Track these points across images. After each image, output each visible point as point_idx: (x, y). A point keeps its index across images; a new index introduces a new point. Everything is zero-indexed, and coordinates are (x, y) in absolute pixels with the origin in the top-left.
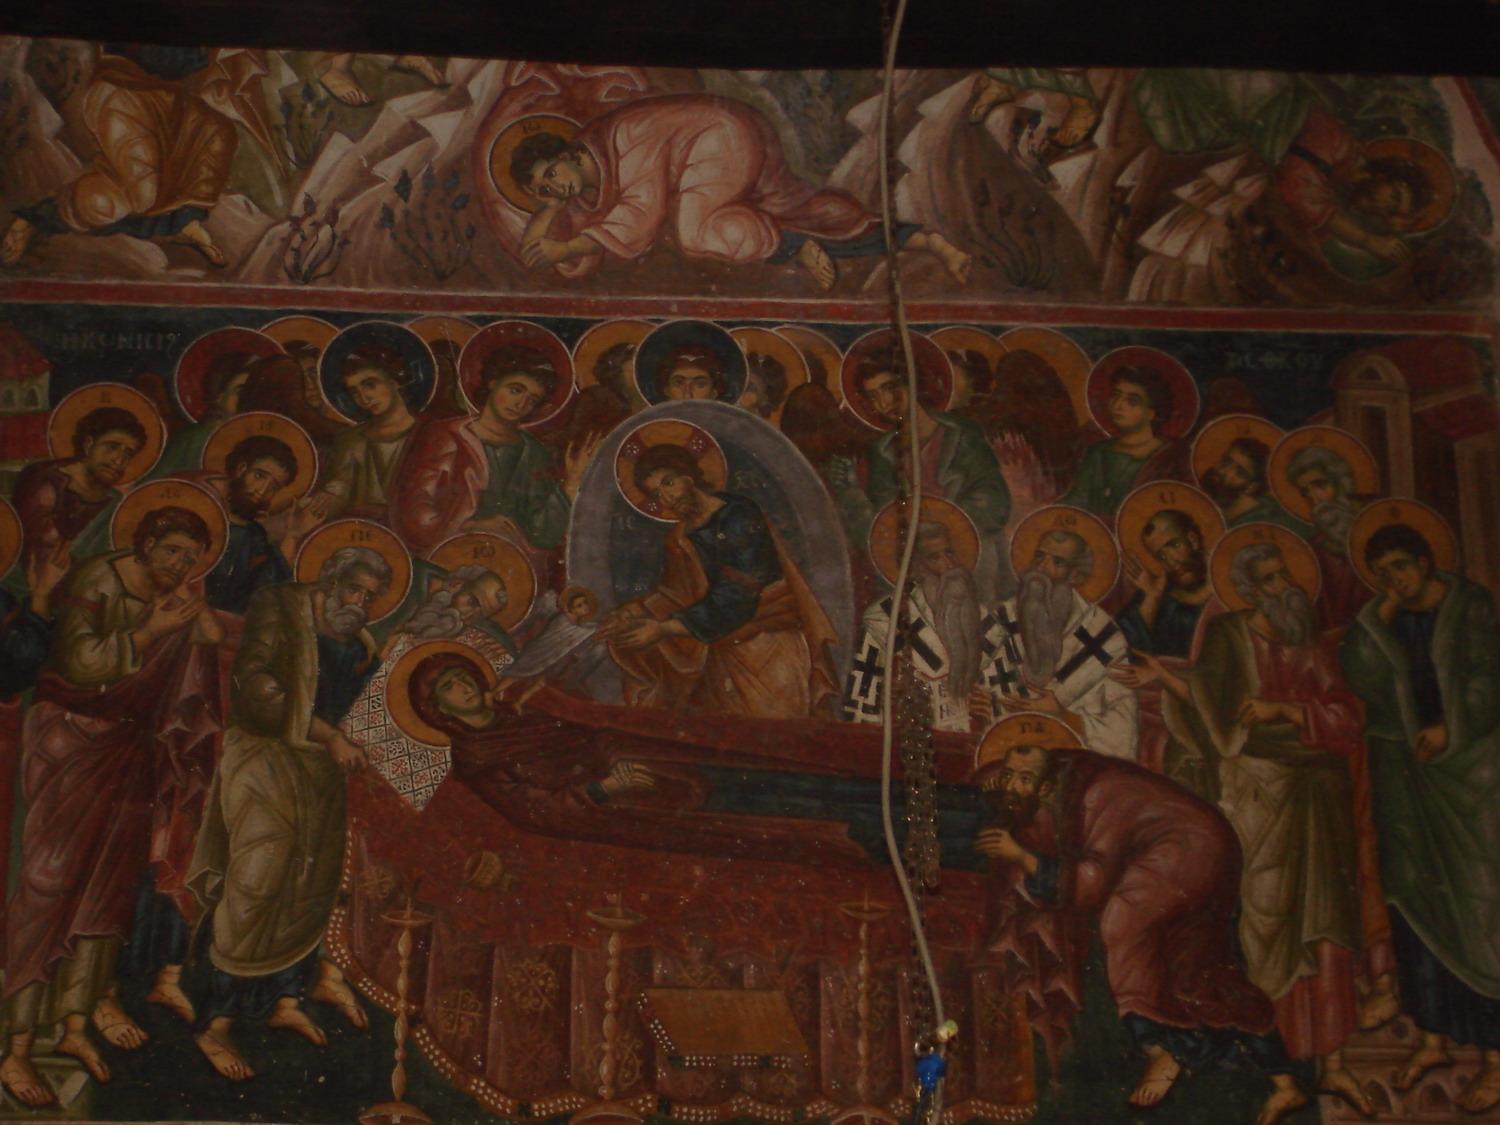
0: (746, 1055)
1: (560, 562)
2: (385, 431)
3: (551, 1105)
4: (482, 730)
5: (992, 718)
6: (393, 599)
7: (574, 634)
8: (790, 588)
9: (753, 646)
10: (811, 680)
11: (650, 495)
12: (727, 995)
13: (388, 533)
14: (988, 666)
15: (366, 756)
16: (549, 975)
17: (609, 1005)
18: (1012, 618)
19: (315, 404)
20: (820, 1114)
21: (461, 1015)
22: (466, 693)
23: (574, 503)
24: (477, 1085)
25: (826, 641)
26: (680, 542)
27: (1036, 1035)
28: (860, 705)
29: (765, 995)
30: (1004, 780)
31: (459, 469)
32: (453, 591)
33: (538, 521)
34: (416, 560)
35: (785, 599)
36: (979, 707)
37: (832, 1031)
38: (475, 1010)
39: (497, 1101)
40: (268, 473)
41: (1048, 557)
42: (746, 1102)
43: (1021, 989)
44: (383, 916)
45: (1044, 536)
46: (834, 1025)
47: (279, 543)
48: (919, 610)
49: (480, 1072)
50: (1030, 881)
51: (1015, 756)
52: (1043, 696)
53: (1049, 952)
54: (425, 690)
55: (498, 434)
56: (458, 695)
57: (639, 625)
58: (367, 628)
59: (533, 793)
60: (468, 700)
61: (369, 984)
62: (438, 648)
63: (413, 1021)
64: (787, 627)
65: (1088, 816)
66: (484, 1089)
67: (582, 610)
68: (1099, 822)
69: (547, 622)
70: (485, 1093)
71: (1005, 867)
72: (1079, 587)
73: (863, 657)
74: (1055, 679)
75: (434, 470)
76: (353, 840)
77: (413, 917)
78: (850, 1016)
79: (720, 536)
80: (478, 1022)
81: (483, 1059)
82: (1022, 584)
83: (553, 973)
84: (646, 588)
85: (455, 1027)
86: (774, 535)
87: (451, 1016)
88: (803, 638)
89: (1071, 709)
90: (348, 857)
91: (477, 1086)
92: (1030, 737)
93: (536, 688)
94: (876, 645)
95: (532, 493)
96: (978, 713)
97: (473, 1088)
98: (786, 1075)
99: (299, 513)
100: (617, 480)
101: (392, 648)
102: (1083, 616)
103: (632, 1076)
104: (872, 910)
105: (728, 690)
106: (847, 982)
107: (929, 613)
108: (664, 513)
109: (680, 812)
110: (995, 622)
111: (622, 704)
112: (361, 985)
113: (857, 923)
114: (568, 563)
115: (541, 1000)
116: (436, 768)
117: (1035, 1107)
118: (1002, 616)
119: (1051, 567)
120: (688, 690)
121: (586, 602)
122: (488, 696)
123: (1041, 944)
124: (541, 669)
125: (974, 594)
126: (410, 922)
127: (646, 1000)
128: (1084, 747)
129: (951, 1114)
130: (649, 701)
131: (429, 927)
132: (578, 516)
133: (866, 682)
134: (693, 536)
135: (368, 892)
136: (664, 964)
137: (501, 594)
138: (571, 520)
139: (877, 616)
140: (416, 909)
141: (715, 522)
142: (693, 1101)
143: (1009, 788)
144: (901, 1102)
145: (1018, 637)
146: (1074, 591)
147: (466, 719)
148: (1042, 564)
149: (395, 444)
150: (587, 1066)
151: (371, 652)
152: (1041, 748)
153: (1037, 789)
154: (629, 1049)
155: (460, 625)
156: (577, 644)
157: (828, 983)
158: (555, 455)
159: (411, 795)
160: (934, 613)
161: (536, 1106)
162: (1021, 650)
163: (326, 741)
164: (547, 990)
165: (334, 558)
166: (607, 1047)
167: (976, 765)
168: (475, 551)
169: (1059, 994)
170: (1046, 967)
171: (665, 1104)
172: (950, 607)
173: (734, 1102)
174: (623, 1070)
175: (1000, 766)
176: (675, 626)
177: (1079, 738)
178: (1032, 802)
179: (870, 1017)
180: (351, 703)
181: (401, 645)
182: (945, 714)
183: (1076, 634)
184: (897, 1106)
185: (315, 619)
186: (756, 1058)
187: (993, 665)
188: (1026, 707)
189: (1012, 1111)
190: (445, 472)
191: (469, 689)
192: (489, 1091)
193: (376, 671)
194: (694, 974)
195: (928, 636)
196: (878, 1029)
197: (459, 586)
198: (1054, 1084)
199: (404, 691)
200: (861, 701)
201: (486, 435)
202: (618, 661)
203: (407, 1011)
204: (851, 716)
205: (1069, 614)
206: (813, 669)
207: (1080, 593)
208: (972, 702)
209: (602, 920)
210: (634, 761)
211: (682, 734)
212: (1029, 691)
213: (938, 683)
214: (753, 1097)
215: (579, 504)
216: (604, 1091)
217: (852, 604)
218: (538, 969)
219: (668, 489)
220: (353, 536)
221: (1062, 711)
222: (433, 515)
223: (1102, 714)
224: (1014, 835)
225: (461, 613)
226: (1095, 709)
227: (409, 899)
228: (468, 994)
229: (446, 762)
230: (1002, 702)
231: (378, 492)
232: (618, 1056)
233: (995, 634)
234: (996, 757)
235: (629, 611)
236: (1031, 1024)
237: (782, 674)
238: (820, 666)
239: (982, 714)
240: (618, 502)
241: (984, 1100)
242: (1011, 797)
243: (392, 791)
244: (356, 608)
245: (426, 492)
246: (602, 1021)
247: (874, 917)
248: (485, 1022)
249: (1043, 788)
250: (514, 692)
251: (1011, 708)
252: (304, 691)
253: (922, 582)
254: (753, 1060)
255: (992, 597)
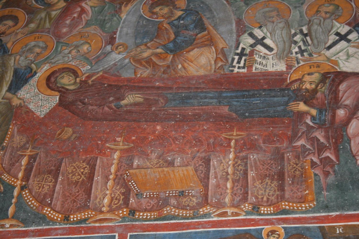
0: (173, 191)
1: (115, 36)
2: (55, 8)
3: (79, 216)
4: (74, 90)
5: (296, 65)
6: (46, 54)
7: (116, 57)
8: (209, 33)
9: (192, 53)
10: (215, 61)
11: (154, 13)
12: (166, 169)
13: (49, 36)
14: (295, 48)
15: (24, 102)
16: (86, 167)
17: (111, 177)
18: (305, 32)
19: (30, 4)
20: (206, 212)
21: (44, 185)
22: (70, 79)
23: (123, 19)
24: (47, 211)
25: (223, 48)
26: (164, 25)
27: (316, 175)
28: (237, 67)
29: (184, 168)
30: (301, 85)
31: (80, 16)
32: (70, 49)
33: (108, 25)
34: (58, 42)
35: (206, 37)
36: (290, 62)
37: (215, 180)
38: (50, 182)
39: (55, 216)
40: (7, 24)
41: (322, 12)
42: (171, 209)
43: (309, 158)
44: (18, 152)
45: (320, 6)
46: (216, 177)
47: (6, 44)
48: (264, 34)
49: (49, 205)
50: (313, 118)
51: (306, 76)
52: (320, 56)
53: (323, 143)
54: (53, 79)
55: (97, 4)
56: (67, 81)
57: (144, 52)
58: (34, 64)
59: (90, 107)
60: (69, 81)
61: (6, 176)
62: (61, 67)
63: (23, 188)
64: (206, 45)
65: (341, 94)
66: (50, 212)
67: (121, 50)
68: (346, 94)
69: (107, 54)
70: (50, 213)
71: (301, 115)
72: (336, 20)
73: (239, 51)
74: (325, 50)
75: (70, 16)
76: (12, 129)
77: (31, 151)
78: (224, 174)
79: (182, 22)
80: (51, 186)
81: (51, 201)
82: (310, 21)
83: (88, 167)
84: (148, 40)
85: (41, 189)
86: (204, 19)
87: (40, 185)
88: (213, 48)
89: (333, 58)
90: (8, 134)
91: (47, 211)
92: (313, 70)
93: (98, 75)
94: (244, 47)
95: (107, 18)
96: (290, 64)
97: (45, 211)
98: (191, 198)
99: (17, 34)
100: (142, 11)
101: (43, 68)
102: (338, 28)
103: (118, 203)
104: (237, 135)
105: (179, 68)
106: (223, 161)
107: (268, 34)
108: (158, 18)
109: (153, 109)
110: (298, 34)
111: (134, 76)
112: (3, 177)
113: (230, 140)
114: (117, 36)
115: (81, 177)
116: (52, 103)
117: (315, 203)
118: (301, 32)
119: (323, 14)
120: (162, 70)
121: (123, 47)
122: (78, 80)
123: (318, 140)
124: (102, 69)
125: (288, 26)
126: (29, 153)
127: (128, 174)
128: (339, 70)
129: (272, 209)
130: (145, 75)
131: (37, 154)
132: (124, 22)
133: (240, 59)
134: (171, 23)
135: (14, 145)
136: (139, 161)
137: (89, 48)
138: (121, 24)
139: (246, 38)
140: (33, 148)
141: (179, 18)
142: (146, 210)
143: (304, 87)
144: (247, 205)
145: (308, 38)
146: (334, 21)
147: (67, 87)
148: (319, 14)
149: (57, 11)
150: (98, 200)
151: (33, 71)
152: (319, 73)
153: (317, 86)
154: (118, 193)
155: (71, 59)
156: (117, 60)
157: (214, 162)
158: (118, 6)
159: (40, 112)
160: (271, 34)
161: (72, 217)
162: (310, 42)
163: (10, 99)
164: (84, 173)
165: (26, 46)
166: (108, 192)
167: (288, 81)
168: (81, 36)
169: (328, 157)
170: (321, 148)
171: (132, 212)
172: (277, 31)
173: (165, 210)
174: (114, 201)
175: (300, 80)
176: (159, 50)
177: (336, 67)
178: (315, 91)
179: (234, 174)
180: (23, 86)
181: (46, 67)
182: (274, 66)
183: (335, 34)
184: (245, 207)
185: (14, 63)
186: (177, 192)
187: (297, 48)
188: (312, 60)
189: (303, 206)
190: (74, 17)
191: (71, 78)
192: (52, 212)
193: (34, 76)
194: (152, 163)
195: (268, 41)
196: (238, 178)
197: (72, 48)
198: (325, 193)
199: (45, 82)
200: (237, 65)
201: (92, 4)
202: (134, 64)
203: (21, 185)
204: (232, 71)
205: (332, 28)
206: (217, 57)
207: (338, 22)
208: (287, 61)
209: (112, 147)
210: (135, 94)
211: (158, 84)
212: (313, 55)
213: (271, 56)
214: (174, 207)
215: (125, 19)
216: (104, 209)
217: (235, 35)
218: (81, 166)
219: (162, 11)
220: (35, 38)
221: (328, 59)
222: (67, 29)
223: (347, 59)
224: (306, 103)
225: (72, 55)
226: (345, 57)
227: (31, 146)
228: (49, 176)
229: (56, 101)
230: (300, 59)
231: (47, 25)
232: (113, 195)
233: (298, 38)
234: (297, 78)
235: (141, 48)
236: (313, 171)
237: (203, 60)
238: (220, 56)
239: (291, 64)
240: (141, 16)
241: (289, 202)
242: (304, 90)
243: (33, 112)
244: (31, 58)
245: (66, 24)
246: (107, 182)
247: (237, 138)
248: (55, 186)
249: (320, 86)
250: (89, 77)
251: (304, 61)
252: (5, 85)
253: (266, 25)
254: (176, 193)
255: (296, 27)
